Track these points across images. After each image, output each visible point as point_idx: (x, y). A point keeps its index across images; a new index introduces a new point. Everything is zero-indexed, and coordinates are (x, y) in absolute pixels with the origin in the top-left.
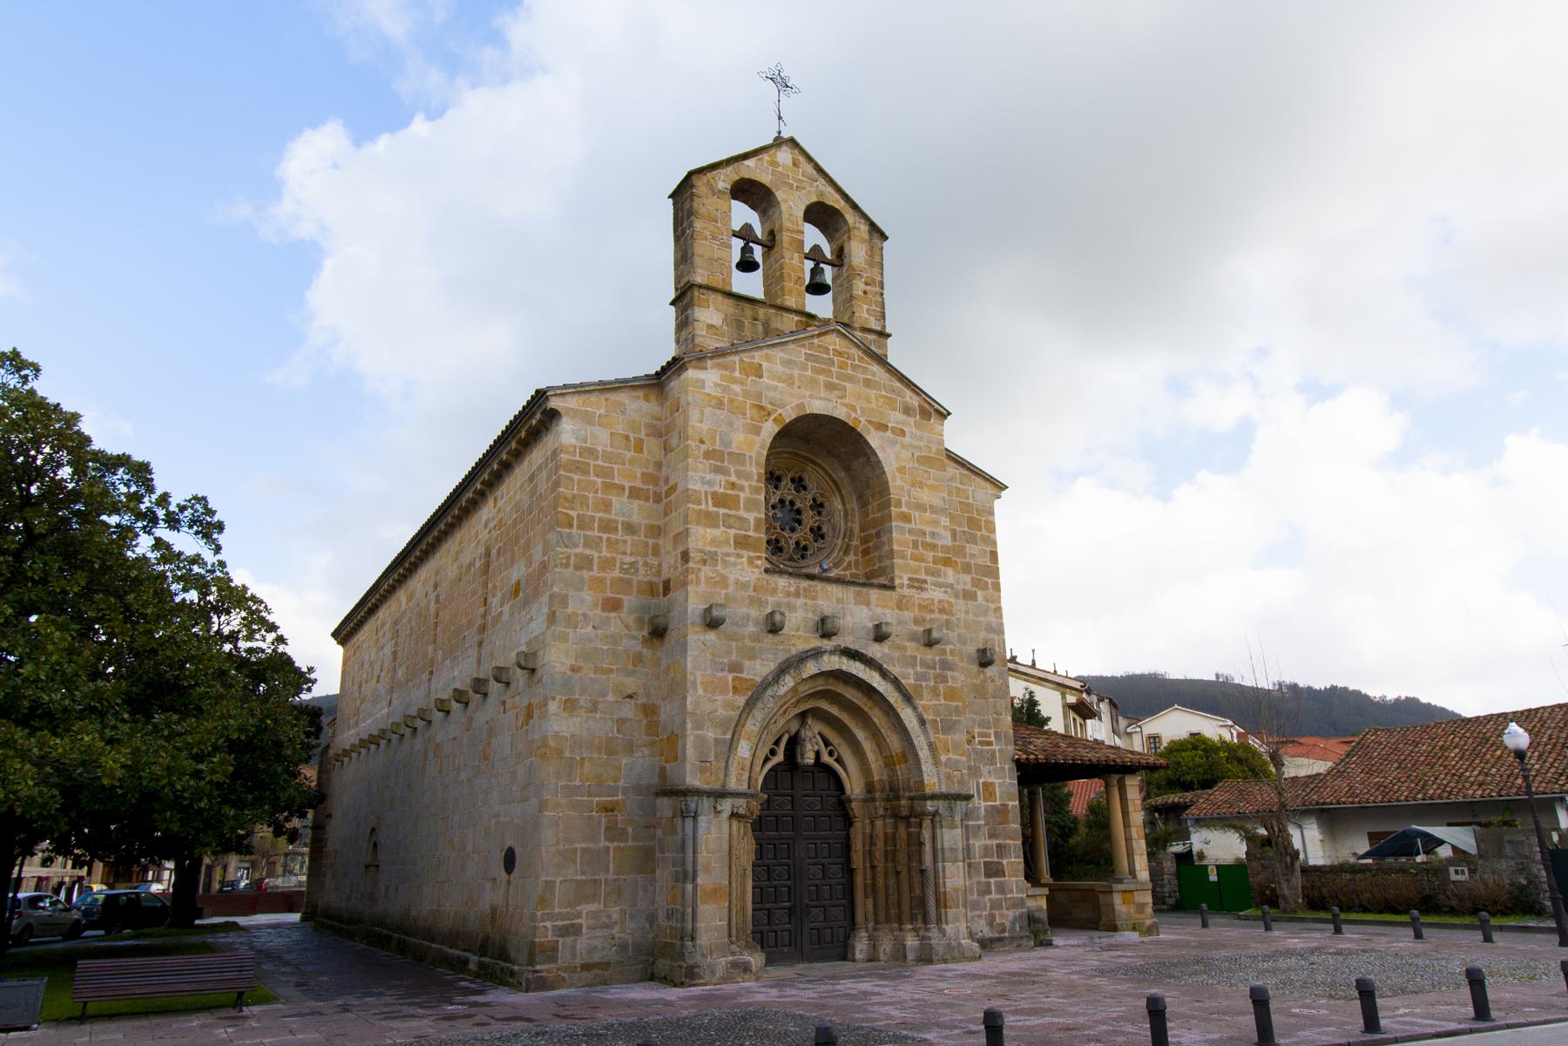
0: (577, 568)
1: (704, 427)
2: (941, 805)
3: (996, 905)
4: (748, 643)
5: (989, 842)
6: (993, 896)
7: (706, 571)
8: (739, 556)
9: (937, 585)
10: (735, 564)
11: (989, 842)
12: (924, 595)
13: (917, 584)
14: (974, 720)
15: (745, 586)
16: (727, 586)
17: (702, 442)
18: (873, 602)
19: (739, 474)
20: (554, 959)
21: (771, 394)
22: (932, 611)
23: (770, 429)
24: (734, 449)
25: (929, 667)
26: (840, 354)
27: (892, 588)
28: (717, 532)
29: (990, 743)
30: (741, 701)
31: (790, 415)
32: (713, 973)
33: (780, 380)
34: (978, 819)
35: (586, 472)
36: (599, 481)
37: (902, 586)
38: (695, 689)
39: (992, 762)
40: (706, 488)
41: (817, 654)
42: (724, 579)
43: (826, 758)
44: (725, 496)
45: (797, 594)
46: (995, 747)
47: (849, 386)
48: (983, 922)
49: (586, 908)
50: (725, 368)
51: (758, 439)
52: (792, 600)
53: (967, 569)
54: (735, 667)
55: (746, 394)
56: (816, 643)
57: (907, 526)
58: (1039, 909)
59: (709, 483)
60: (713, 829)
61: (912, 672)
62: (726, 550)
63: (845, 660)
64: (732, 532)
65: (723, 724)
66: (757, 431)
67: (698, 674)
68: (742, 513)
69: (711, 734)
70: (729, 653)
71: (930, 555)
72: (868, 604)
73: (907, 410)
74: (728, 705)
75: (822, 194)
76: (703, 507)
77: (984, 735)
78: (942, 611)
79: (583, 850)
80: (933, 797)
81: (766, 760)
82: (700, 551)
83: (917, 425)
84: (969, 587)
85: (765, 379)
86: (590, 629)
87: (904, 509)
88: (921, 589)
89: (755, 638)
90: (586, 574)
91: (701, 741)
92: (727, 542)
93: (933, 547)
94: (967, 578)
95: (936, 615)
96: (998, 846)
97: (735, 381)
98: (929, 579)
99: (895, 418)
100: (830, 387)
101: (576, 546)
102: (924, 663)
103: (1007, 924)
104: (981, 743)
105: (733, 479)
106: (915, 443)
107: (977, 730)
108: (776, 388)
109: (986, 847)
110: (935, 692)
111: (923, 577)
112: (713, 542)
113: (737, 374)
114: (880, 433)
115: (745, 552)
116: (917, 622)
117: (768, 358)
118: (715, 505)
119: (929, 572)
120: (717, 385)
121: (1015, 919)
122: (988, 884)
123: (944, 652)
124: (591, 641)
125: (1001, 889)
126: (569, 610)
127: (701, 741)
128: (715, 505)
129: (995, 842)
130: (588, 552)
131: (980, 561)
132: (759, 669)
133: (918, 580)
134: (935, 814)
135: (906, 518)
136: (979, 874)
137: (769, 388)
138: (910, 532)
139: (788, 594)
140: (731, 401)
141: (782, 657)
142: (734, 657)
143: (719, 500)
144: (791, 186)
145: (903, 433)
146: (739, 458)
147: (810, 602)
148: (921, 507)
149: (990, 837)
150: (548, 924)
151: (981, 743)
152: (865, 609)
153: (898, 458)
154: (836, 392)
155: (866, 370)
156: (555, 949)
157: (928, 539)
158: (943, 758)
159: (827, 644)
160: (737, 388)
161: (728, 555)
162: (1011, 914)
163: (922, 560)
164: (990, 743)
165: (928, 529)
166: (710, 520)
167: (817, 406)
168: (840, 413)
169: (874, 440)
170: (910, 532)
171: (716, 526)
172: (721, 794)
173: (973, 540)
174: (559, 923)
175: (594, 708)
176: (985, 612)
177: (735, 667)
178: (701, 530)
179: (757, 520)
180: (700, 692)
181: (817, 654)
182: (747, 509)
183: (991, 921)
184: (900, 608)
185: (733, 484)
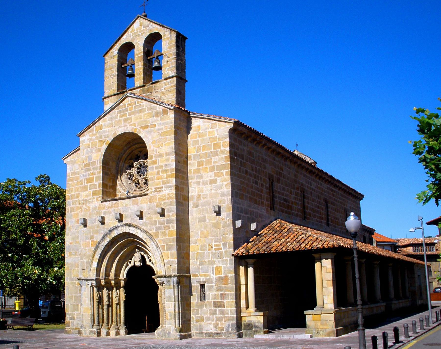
0: (71, 212)
1: (84, 157)
2: (164, 280)
3: (218, 319)
4: (95, 228)
5: (217, 293)
6: (218, 316)
7: (84, 207)
8: (94, 198)
9: (166, 188)
10: (92, 202)
11: (217, 293)
12: (161, 193)
13: (158, 190)
14: (212, 240)
15: (94, 209)
16: (90, 210)
17: (83, 162)
18: (139, 202)
19: (94, 169)
20: (69, 326)
21: (105, 134)
22: (164, 199)
23: (105, 147)
24: (93, 161)
25: (162, 224)
26: (130, 105)
27: (147, 195)
28: (87, 192)
29: (221, 249)
30: (93, 248)
31: (110, 139)
32: (86, 333)
33: (108, 126)
34: (212, 282)
35: (72, 180)
36: (76, 182)
37: (151, 192)
38: (81, 246)
39: (221, 256)
40: (85, 178)
41: (116, 228)
42: (89, 207)
43: (148, 263)
44: (89, 178)
45: (112, 207)
46: (223, 250)
47: (133, 116)
48: (212, 327)
49: (76, 312)
50: (90, 132)
51: (100, 153)
52: (110, 210)
53: (212, 169)
54: (92, 238)
55: (97, 138)
56: (117, 223)
57: (154, 166)
58: (259, 322)
59: (85, 176)
60: (86, 290)
61: (154, 227)
62: (90, 197)
63: (127, 227)
64: (92, 191)
65: (88, 257)
66: (99, 150)
67: (81, 241)
68: (95, 183)
69: (85, 261)
70: (90, 233)
71: (165, 175)
72: (137, 204)
73: (157, 114)
74: (90, 251)
75: (151, 30)
76: (83, 185)
77: (217, 245)
78: (168, 199)
79: (75, 296)
80: (159, 277)
81: (127, 265)
82: (82, 200)
83: (161, 119)
84: (213, 178)
85: (103, 129)
86: (74, 230)
87: (154, 159)
88: (160, 191)
89: (98, 226)
90: (73, 213)
91: (83, 263)
92: (90, 195)
93: (166, 171)
94: (212, 173)
95: (166, 201)
96: (221, 294)
97: (93, 135)
98: (163, 186)
99: (152, 120)
100: (126, 120)
101: (70, 205)
102: (160, 223)
103: (225, 328)
104: (215, 249)
105: (92, 171)
106: (160, 127)
107: (213, 244)
108: (106, 131)
109: (215, 295)
110: (164, 234)
111: (161, 186)
112: (87, 196)
113: (94, 132)
114: (145, 130)
115: (95, 197)
116: (157, 206)
117: (104, 121)
118: (87, 183)
119: (164, 183)
120: (88, 139)
121: (229, 326)
122: (216, 311)
123: (169, 216)
124: (74, 234)
125: (222, 313)
126: (69, 225)
127: (83, 263)
128: (87, 183)
129: (220, 293)
130: (73, 206)
131: (219, 164)
132: (98, 237)
133: (158, 188)
134: (162, 283)
135: (155, 162)
136: (211, 306)
137: (104, 132)
138: (156, 168)
139: (109, 208)
140: (92, 143)
141: (106, 231)
142: (91, 234)
143: (89, 181)
144: (139, 35)
145: (155, 125)
146: (93, 163)
147: (116, 209)
148: (161, 155)
149: (218, 290)
150: (68, 316)
151: (215, 249)
152: (136, 206)
153: (152, 138)
154: (128, 122)
155: (139, 106)
156: (69, 323)
157: (164, 168)
158: (166, 261)
159: (121, 224)
160: (94, 137)
161: (90, 199)
162: (227, 323)
163: (162, 178)
164: (221, 249)
165: (163, 164)
166: (85, 189)
167: (120, 131)
168: (129, 129)
169: (142, 135)
170: (156, 168)
171: (87, 190)
172: (87, 280)
173: (216, 154)
174: (70, 316)
175: (76, 255)
176: (221, 187)
177: (92, 238)
178: (83, 193)
179: (99, 183)
180: (82, 247)
181: (116, 228)
182: (96, 181)
183: (216, 326)
184: (150, 202)
185: (92, 173)
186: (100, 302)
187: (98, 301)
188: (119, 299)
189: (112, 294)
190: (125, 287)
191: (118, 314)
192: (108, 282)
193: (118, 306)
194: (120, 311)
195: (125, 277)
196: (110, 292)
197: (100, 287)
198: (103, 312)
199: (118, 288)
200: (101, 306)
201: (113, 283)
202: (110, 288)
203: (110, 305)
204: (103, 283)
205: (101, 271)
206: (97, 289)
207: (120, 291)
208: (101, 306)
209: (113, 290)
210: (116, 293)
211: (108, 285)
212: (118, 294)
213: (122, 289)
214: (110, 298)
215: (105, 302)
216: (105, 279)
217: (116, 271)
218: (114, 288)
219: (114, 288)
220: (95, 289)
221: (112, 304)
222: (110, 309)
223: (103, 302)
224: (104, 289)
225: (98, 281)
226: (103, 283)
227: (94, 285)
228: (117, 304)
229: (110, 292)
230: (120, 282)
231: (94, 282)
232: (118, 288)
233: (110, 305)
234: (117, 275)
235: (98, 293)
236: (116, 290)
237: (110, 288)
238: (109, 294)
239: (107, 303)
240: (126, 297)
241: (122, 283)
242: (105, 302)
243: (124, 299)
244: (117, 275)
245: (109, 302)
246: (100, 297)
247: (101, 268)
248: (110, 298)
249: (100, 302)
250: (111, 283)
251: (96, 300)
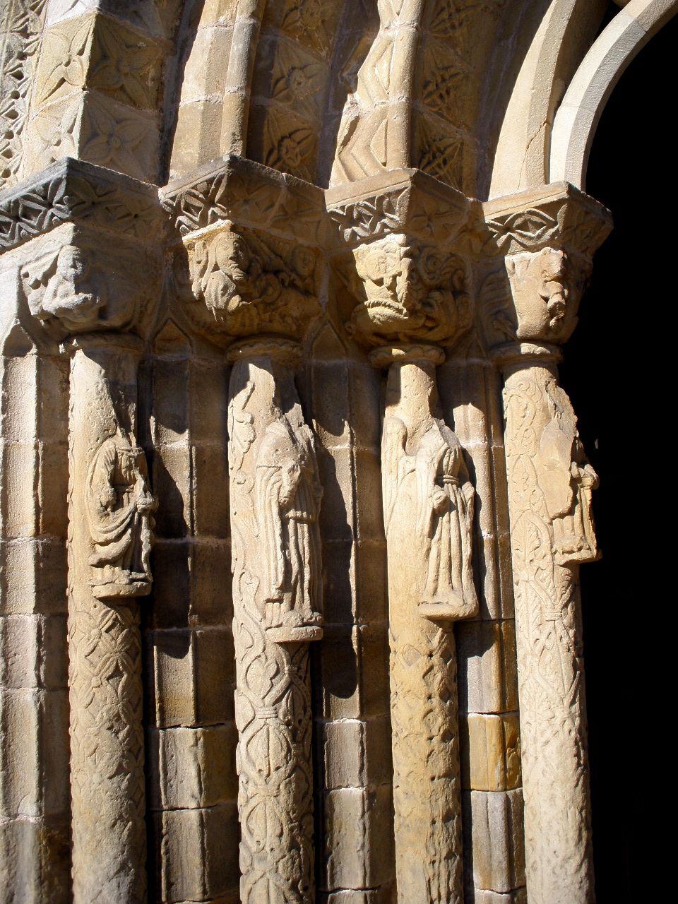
186: (174, 593)
187: (118, 581)
188: (488, 558)
189: (369, 463)
190: (578, 361)
191: (487, 805)
192: (295, 273)
193: (481, 670)
194: (510, 743)
195: (568, 167)
196: (341, 448)
197: (159, 356)
198: (221, 777)
199: (468, 378)
200: (180, 676)
201: (382, 264)
202: (336, 379)
203: (339, 660)
204: (211, 262)
205: (192, 92)
206: (114, 388)
207: (495, 423)
208: (180, 676)
209: (387, 393)
210: (433, 442)
211: (294, 305)
212: (463, 470)
213: (531, 396)
214: (337, 539)
215: (263, 617)
216: (239, 184)
217: (424, 82)
218: (413, 382)
219: (413, 382)
220: (85, 375)
221: (378, 645)
222: (347, 722)
223: (223, 610)
224: (230, 382)
225: (104, 197)
226: (211, 262)
227: (60, 295)
228: (474, 633)
229: (341, 448)
230: (497, 281)
231: (57, 244)
232: (468, 378)
233: (339, 660)
234: (448, 148)
235: (123, 445)
236: (441, 408)
237: (336, 379)
238: (317, 467)
239: (293, 622)
240: (605, 513)
241: (534, 283)
242: (263, 617)
243: (577, 538)
244: (448, 148)
245: (330, 599)
246: (165, 514)
247: (180, 46)
248: (337, 539)
249: (174, 593)
250: (348, 291)
251: (91, 585)
